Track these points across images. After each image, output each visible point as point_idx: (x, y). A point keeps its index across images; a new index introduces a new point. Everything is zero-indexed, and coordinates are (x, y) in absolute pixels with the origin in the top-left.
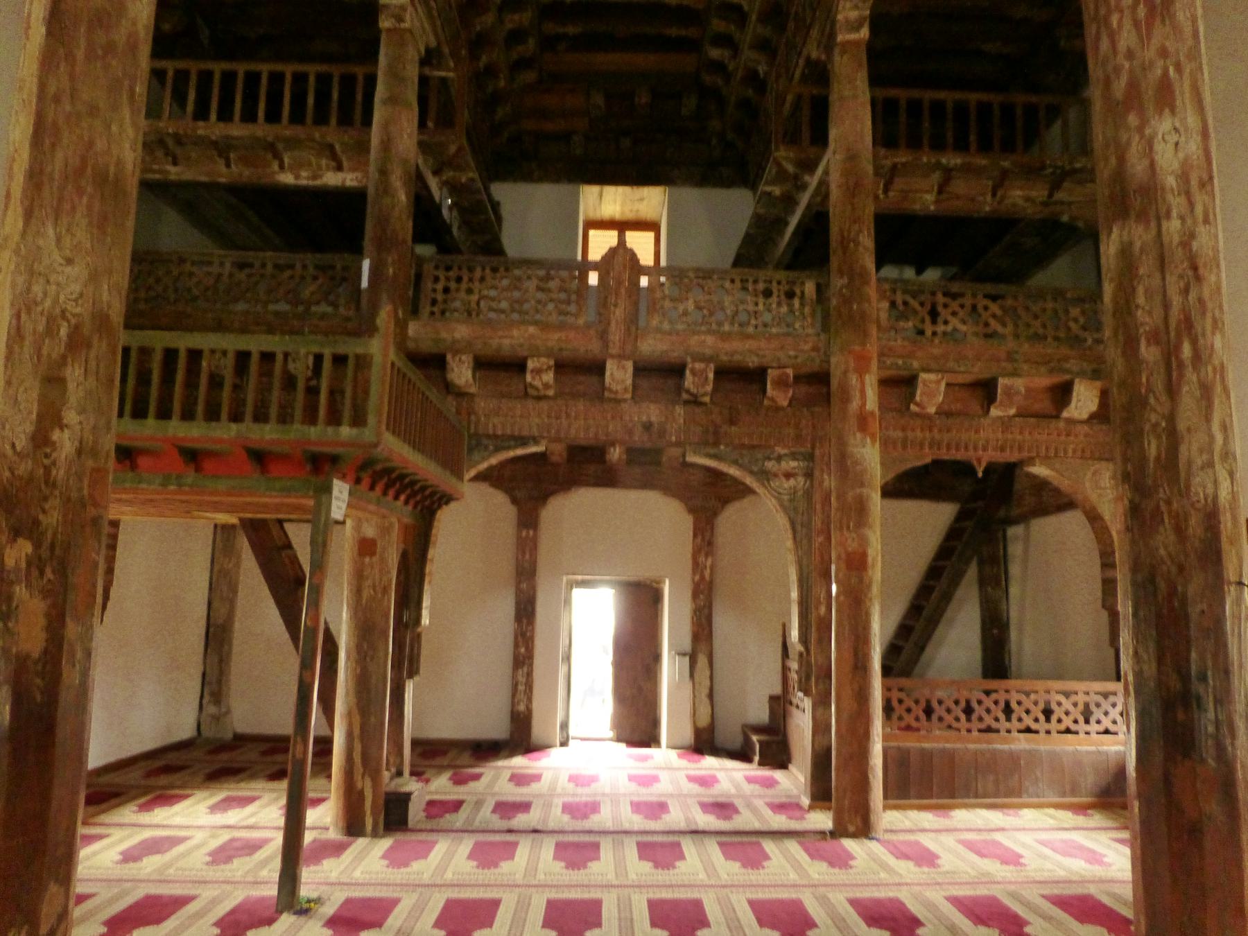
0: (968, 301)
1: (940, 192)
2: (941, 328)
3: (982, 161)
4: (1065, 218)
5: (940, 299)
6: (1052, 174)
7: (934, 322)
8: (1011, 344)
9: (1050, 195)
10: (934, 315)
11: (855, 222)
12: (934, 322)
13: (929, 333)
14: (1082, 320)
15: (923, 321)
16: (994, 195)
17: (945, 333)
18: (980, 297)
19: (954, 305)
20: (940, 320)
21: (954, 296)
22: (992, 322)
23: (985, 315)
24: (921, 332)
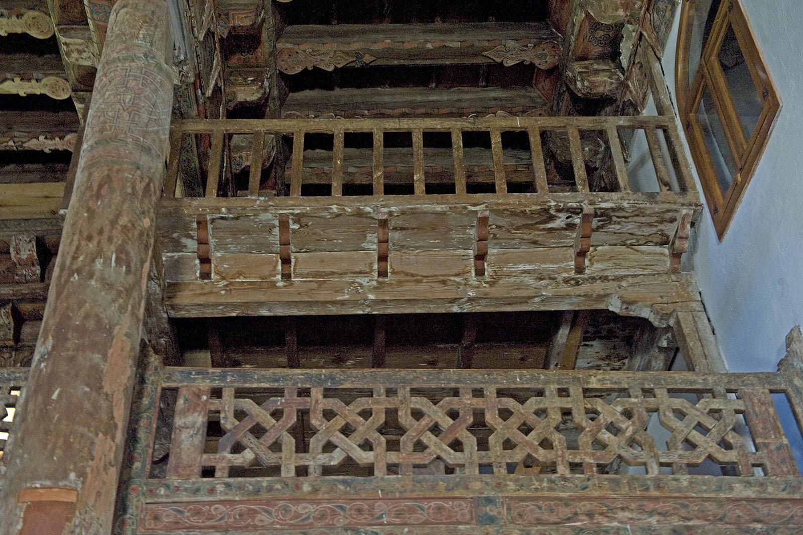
0: (379, 405)
1: (383, 273)
2: (316, 459)
3: (436, 205)
4: (615, 306)
5: (318, 400)
6: (570, 227)
7: (302, 447)
8: (478, 485)
9: (580, 270)
10: (302, 433)
11: (90, 238)
12: (302, 447)
13: (287, 472)
14: (629, 428)
15: (276, 447)
16: (480, 272)
17: (327, 471)
18: (404, 392)
19: (349, 413)
20: (315, 443)
21: (348, 396)
22: (429, 438)
23: (414, 429)
24: (275, 470)
